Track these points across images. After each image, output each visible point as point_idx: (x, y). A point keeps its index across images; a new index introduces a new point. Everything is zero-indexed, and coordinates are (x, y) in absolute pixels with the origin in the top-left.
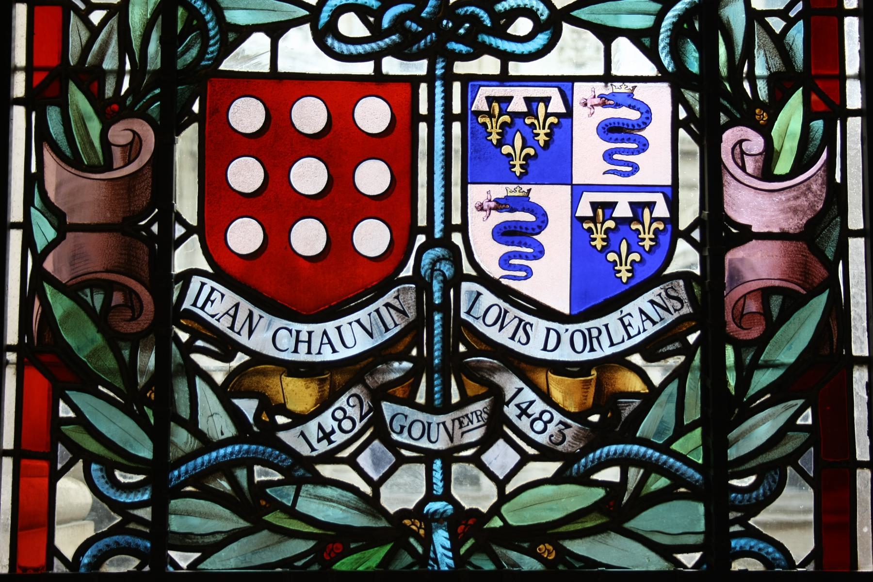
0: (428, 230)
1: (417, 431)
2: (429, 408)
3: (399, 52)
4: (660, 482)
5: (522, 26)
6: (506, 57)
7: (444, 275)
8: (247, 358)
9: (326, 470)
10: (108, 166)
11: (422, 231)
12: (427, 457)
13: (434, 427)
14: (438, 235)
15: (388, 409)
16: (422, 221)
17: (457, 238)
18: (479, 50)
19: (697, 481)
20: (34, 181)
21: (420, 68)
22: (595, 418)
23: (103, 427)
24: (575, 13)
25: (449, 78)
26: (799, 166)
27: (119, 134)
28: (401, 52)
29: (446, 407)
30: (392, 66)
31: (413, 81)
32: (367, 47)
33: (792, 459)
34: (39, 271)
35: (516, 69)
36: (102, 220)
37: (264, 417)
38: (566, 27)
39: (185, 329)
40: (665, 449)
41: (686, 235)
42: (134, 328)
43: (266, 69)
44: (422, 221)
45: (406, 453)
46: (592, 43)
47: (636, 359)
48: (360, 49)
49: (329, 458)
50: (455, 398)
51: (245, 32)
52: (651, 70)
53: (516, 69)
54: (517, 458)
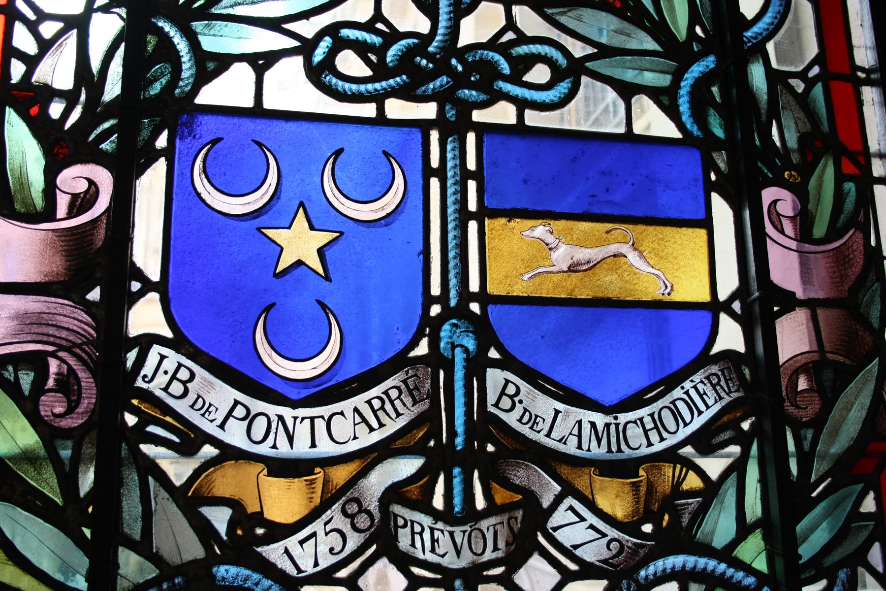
5: (540, 74)
6: (522, 105)
21: (428, 111)
28: (407, 93)
31: (424, 126)
32: (370, 87)
53: (533, 118)
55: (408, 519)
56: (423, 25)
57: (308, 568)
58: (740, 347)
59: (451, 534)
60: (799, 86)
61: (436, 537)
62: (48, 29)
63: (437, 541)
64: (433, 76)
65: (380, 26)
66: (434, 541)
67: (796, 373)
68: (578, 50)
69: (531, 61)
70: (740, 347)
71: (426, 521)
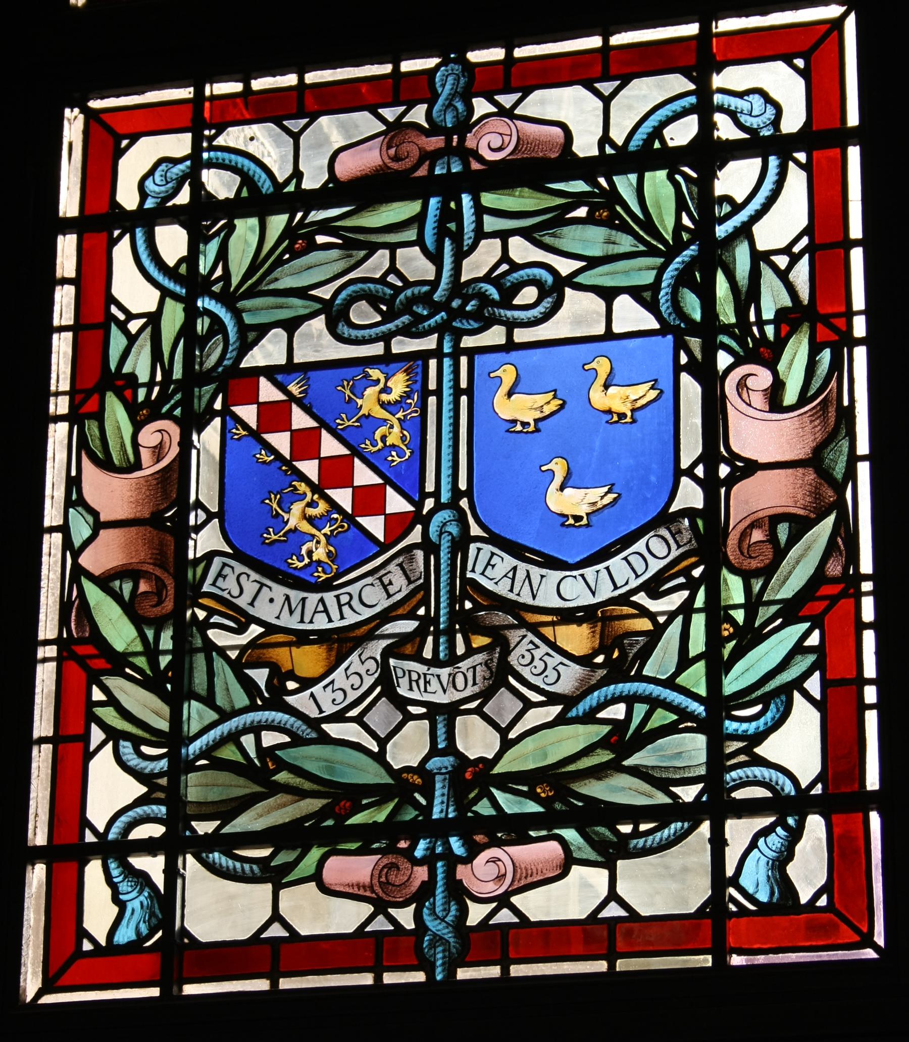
0: (436, 494)
2: (435, 662)
3: (407, 332)
4: (662, 717)
6: (511, 326)
7: (450, 533)
8: (261, 630)
10: (137, 465)
11: (430, 495)
12: (433, 711)
14: (445, 497)
16: (430, 487)
18: (487, 324)
19: (700, 714)
20: (73, 483)
21: (430, 343)
23: (127, 703)
24: (579, 279)
25: (457, 353)
26: (803, 399)
27: (149, 436)
29: (453, 660)
30: (402, 345)
31: (423, 356)
33: (798, 684)
34: (76, 566)
35: (521, 335)
36: (131, 516)
38: (568, 291)
39: (203, 607)
40: (670, 683)
41: (690, 472)
42: (157, 611)
43: (283, 361)
46: (598, 304)
47: (641, 598)
48: (373, 332)
49: (339, 717)
50: (460, 650)
52: (652, 324)
53: (521, 335)
54: (520, 705)
55: (405, 669)
56: (428, 270)
57: (329, 709)
59: (438, 676)
60: (782, 261)
61: (428, 680)
62: (134, 326)
63: (429, 682)
65: (391, 279)
66: (427, 683)
67: (752, 526)
68: (565, 267)
69: (518, 287)
71: (421, 668)
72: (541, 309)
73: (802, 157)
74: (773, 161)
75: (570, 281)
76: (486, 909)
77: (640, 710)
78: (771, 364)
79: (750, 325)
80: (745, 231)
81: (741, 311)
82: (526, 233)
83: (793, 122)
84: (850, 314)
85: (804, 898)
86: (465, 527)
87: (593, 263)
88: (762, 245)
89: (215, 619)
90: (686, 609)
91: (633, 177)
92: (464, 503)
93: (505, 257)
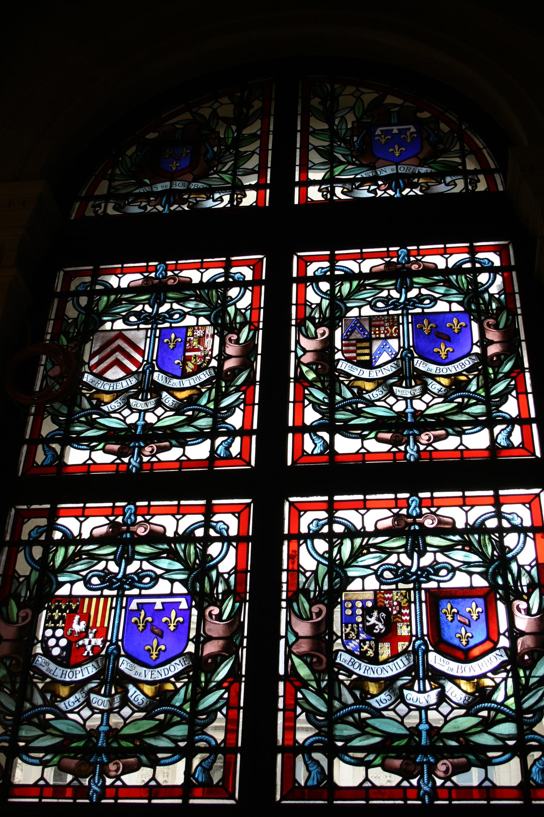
0: (111, 641)
1: (100, 702)
6: (141, 589)
9: (70, 716)
13: (105, 702)
14: (114, 642)
15: (92, 696)
16: (109, 638)
17: (120, 643)
18: (132, 587)
22: (158, 698)
25: (123, 595)
27: (22, 614)
28: (110, 588)
35: (144, 592)
37: (53, 699)
41: (192, 640)
44: (109, 638)
45: (96, 711)
46: (169, 584)
47: (173, 679)
50: (113, 692)
51: (64, 583)
53: (144, 592)
57: (70, 708)
58: (193, 651)
64: (116, 583)
68: (159, 572)
70: (193, 651)
72: (150, 585)
73: (235, 544)
74: (226, 544)
75: (161, 576)
76: (112, 780)
77: (169, 716)
78: (220, 608)
79: (214, 594)
80: (216, 566)
81: (212, 589)
82: (148, 560)
83: (233, 532)
84: (246, 592)
85: (215, 783)
86: (119, 651)
87: (168, 571)
88: (221, 571)
89: (36, 675)
90: (186, 684)
91: (183, 546)
92: (120, 643)
93: (141, 568)
